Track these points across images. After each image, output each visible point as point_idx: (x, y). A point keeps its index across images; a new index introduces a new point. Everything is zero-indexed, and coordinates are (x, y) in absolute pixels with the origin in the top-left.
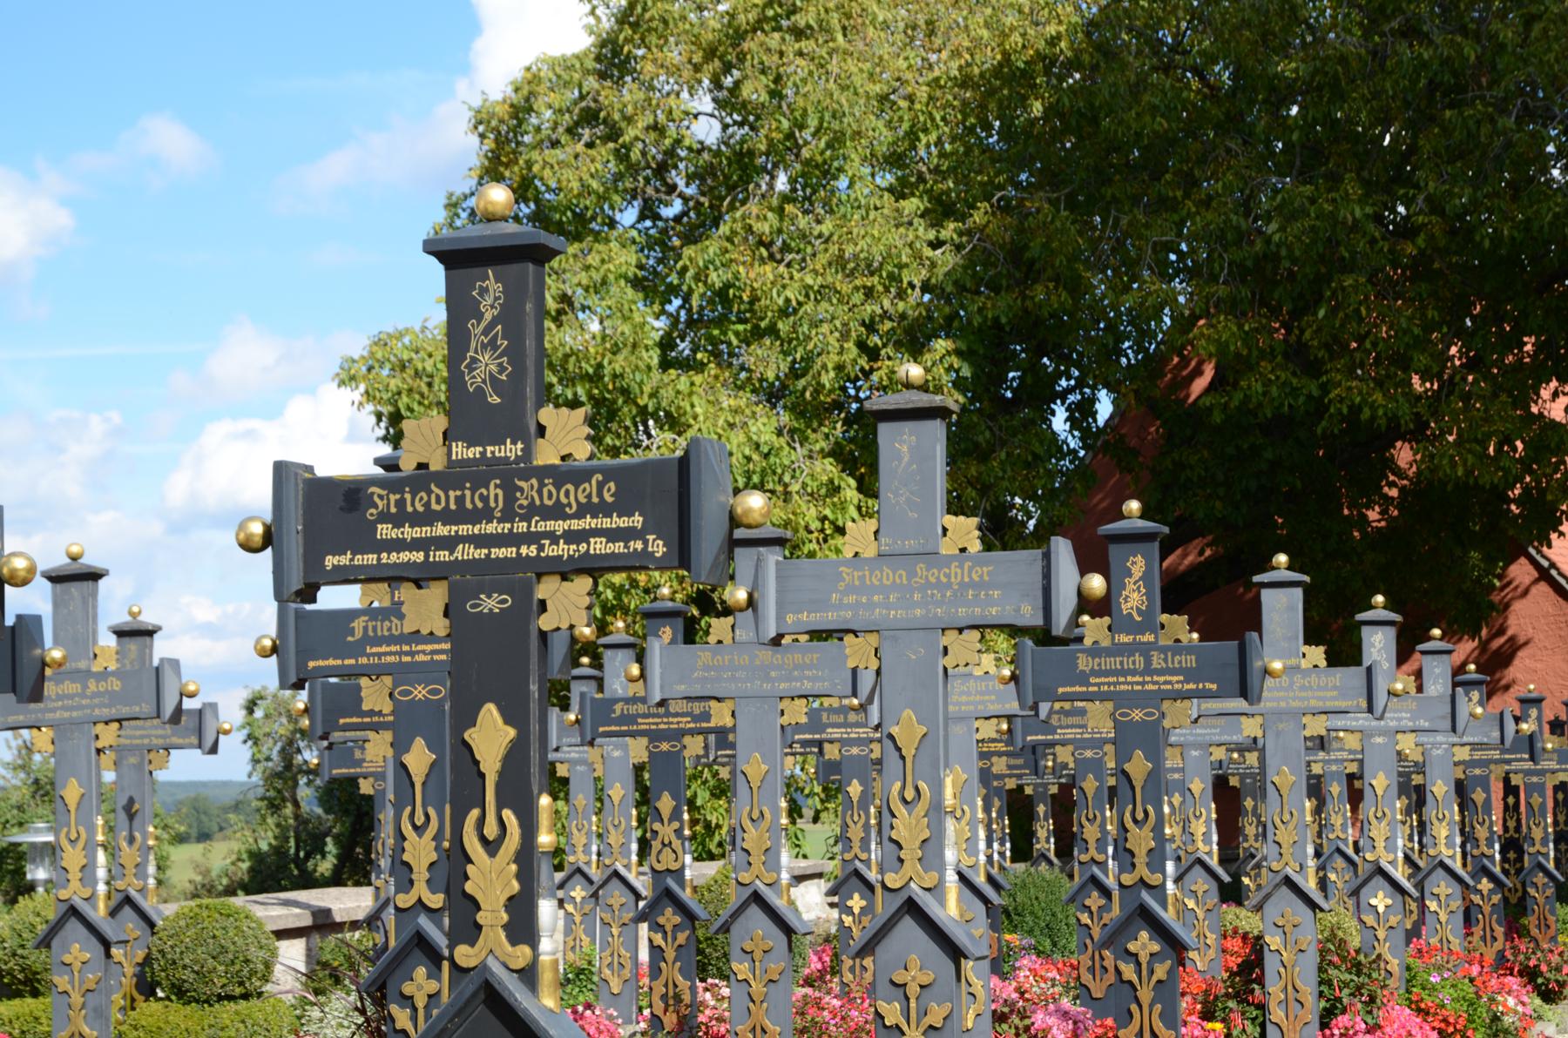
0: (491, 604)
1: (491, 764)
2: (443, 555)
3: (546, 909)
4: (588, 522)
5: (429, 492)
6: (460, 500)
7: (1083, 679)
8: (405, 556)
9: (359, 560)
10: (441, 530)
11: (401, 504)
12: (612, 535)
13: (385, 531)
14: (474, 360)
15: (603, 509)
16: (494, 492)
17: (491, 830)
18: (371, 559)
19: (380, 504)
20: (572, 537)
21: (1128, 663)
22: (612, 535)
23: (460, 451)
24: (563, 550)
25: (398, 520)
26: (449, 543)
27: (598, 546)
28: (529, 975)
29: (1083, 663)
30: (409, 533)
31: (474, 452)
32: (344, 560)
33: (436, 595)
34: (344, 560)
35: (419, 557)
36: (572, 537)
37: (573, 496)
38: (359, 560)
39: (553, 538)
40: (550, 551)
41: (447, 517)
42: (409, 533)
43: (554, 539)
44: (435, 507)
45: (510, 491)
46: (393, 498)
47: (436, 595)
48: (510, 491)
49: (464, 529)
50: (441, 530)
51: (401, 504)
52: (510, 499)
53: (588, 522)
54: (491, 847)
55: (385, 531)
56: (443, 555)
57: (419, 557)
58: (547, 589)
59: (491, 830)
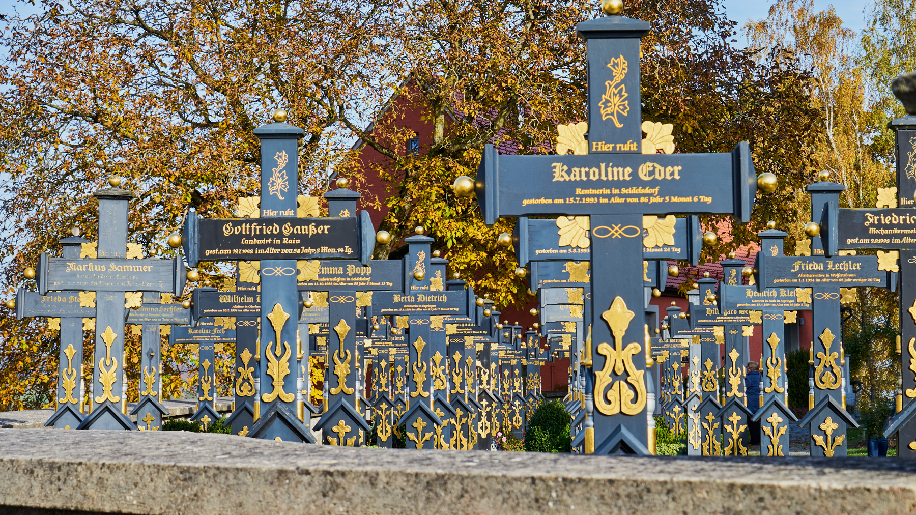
2: (897, 241)
5: (892, 217)
6: (905, 220)
8: (881, 241)
9: (861, 241)
10: (897, 231)
11: (905, 220)
13: (873, 230)
14: (910, 167)
18: (867, 241)
19: (871, 220)
23: (904, 201)
25: (879, 226)
26: (901, 236)
30: (883, 231)
32: (855, 241)
33: (894, 255)
34: (855, 241)
35: (888, 241)
38: (861, 241)
41: (899, 226)
42: (883, 231)
44: (893, 222)
46: (876, 218)
47: (894, 255)
49: (906, 231)
50: (897, 231)
51: (879, 220)
55: (873, 230)
56: (897, 241)
57: (888, 241)
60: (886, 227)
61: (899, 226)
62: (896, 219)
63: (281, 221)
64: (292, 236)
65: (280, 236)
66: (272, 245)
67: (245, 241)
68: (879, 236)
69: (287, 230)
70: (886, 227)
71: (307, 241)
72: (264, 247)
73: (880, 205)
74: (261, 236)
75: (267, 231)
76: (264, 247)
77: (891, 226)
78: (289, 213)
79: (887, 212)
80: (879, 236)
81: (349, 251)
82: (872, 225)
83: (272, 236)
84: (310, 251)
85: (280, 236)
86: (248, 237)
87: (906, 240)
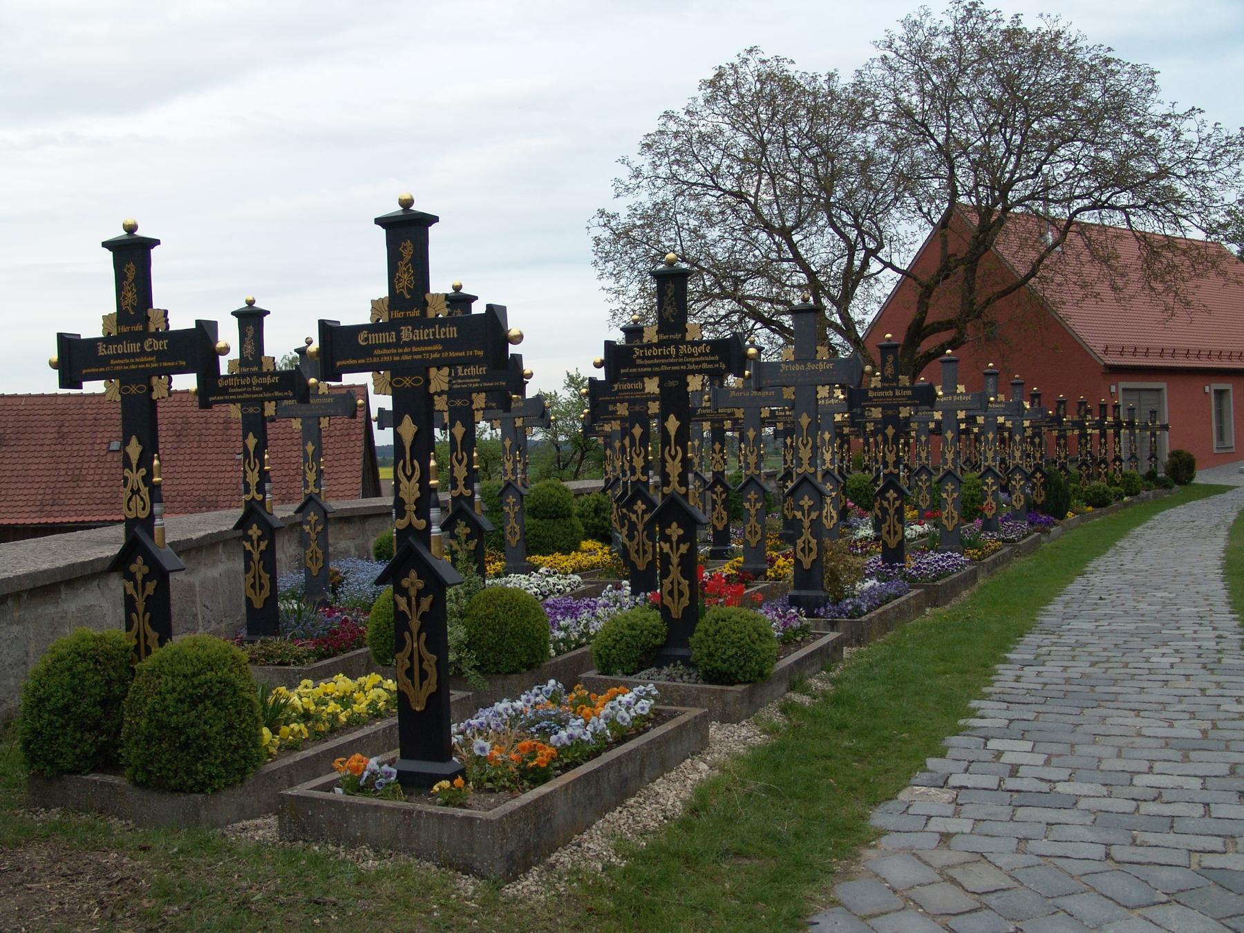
0: (672, 384)
1: (673, 434)
3: (691, 476)
4: (702, 359)
7: (871, 399)
10: (656, 361)
12: (709, 362)
13: (639, 362)
15: (706, 354)
16: (672, 349)
17: (673, 453)
20: (696, 363)
21: (887, 394)
22: (709, 362)
23: (661, 336)
24: (694, 367)
25: (644, 358)
26: (659, 365)
27: (705, 366)
28: (686, 496)
29: (871, 394)
30: (647, 362)
31: (666, 337)
33: (656, 380)
36: (696, 363)
37: (696, 350)
39: (691, 363)
40: (690, 367)
42: (647, 362)
43: (691, 363)
45: (677, 349)
47: (656, 380)
48: (677, 349)
50: (656, 361)
52: (677, 352)
53: (702, 359)
54: (673, 458)
55: (639, 362)
58: (690, 378)
59: (673, 453)
60: (649, 358)
61: (658, 357)
62: (656, 352)
63: (251, 375)
64: (258, 385)
65: (251, 385)
66: (246, 392)
67: (231, 390)
68: (644, 366)
69: (255, 381)
70: (649, 358)
71: (267, 388)
72: (241, 393)
73: (645, 341)
74: (239, 387)
75: (243, 383)
76: (241, 393)
77: (652, 357)
78: (255, 369)
79: (649, 346)
80: (644, 366)
81: (291, 394)
82: (639, 357)
83: (246, 386)
84: (268, 395)
85: (251, 385)
86: (233, 387)
87: (664, 368)
